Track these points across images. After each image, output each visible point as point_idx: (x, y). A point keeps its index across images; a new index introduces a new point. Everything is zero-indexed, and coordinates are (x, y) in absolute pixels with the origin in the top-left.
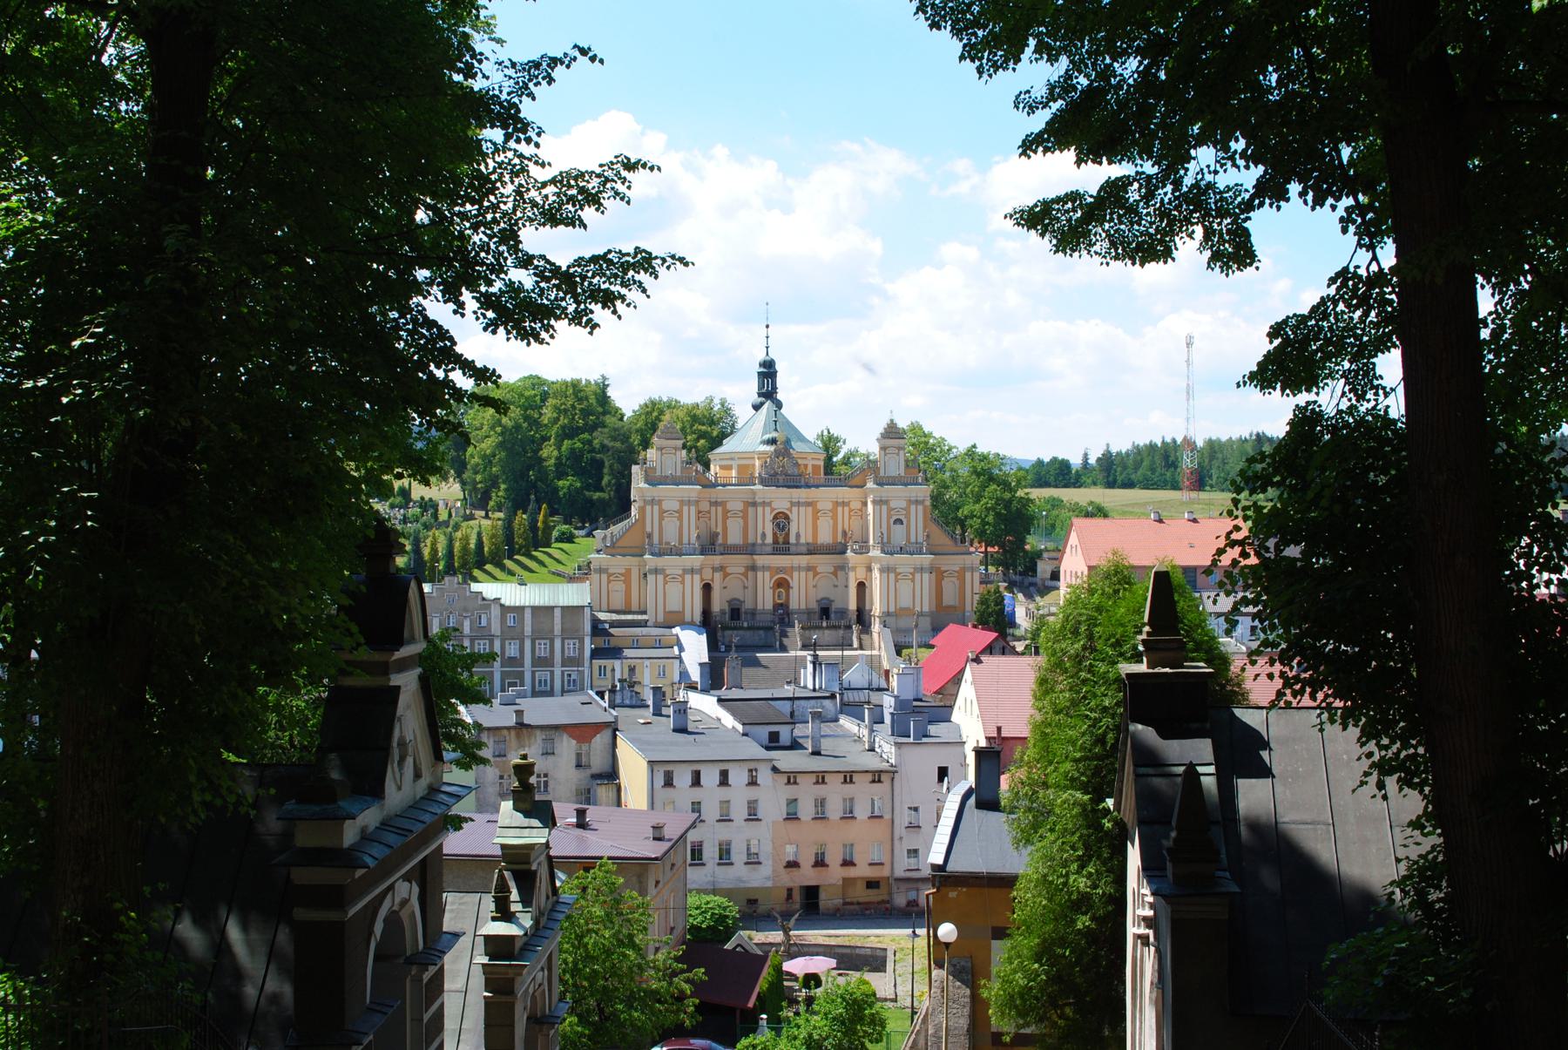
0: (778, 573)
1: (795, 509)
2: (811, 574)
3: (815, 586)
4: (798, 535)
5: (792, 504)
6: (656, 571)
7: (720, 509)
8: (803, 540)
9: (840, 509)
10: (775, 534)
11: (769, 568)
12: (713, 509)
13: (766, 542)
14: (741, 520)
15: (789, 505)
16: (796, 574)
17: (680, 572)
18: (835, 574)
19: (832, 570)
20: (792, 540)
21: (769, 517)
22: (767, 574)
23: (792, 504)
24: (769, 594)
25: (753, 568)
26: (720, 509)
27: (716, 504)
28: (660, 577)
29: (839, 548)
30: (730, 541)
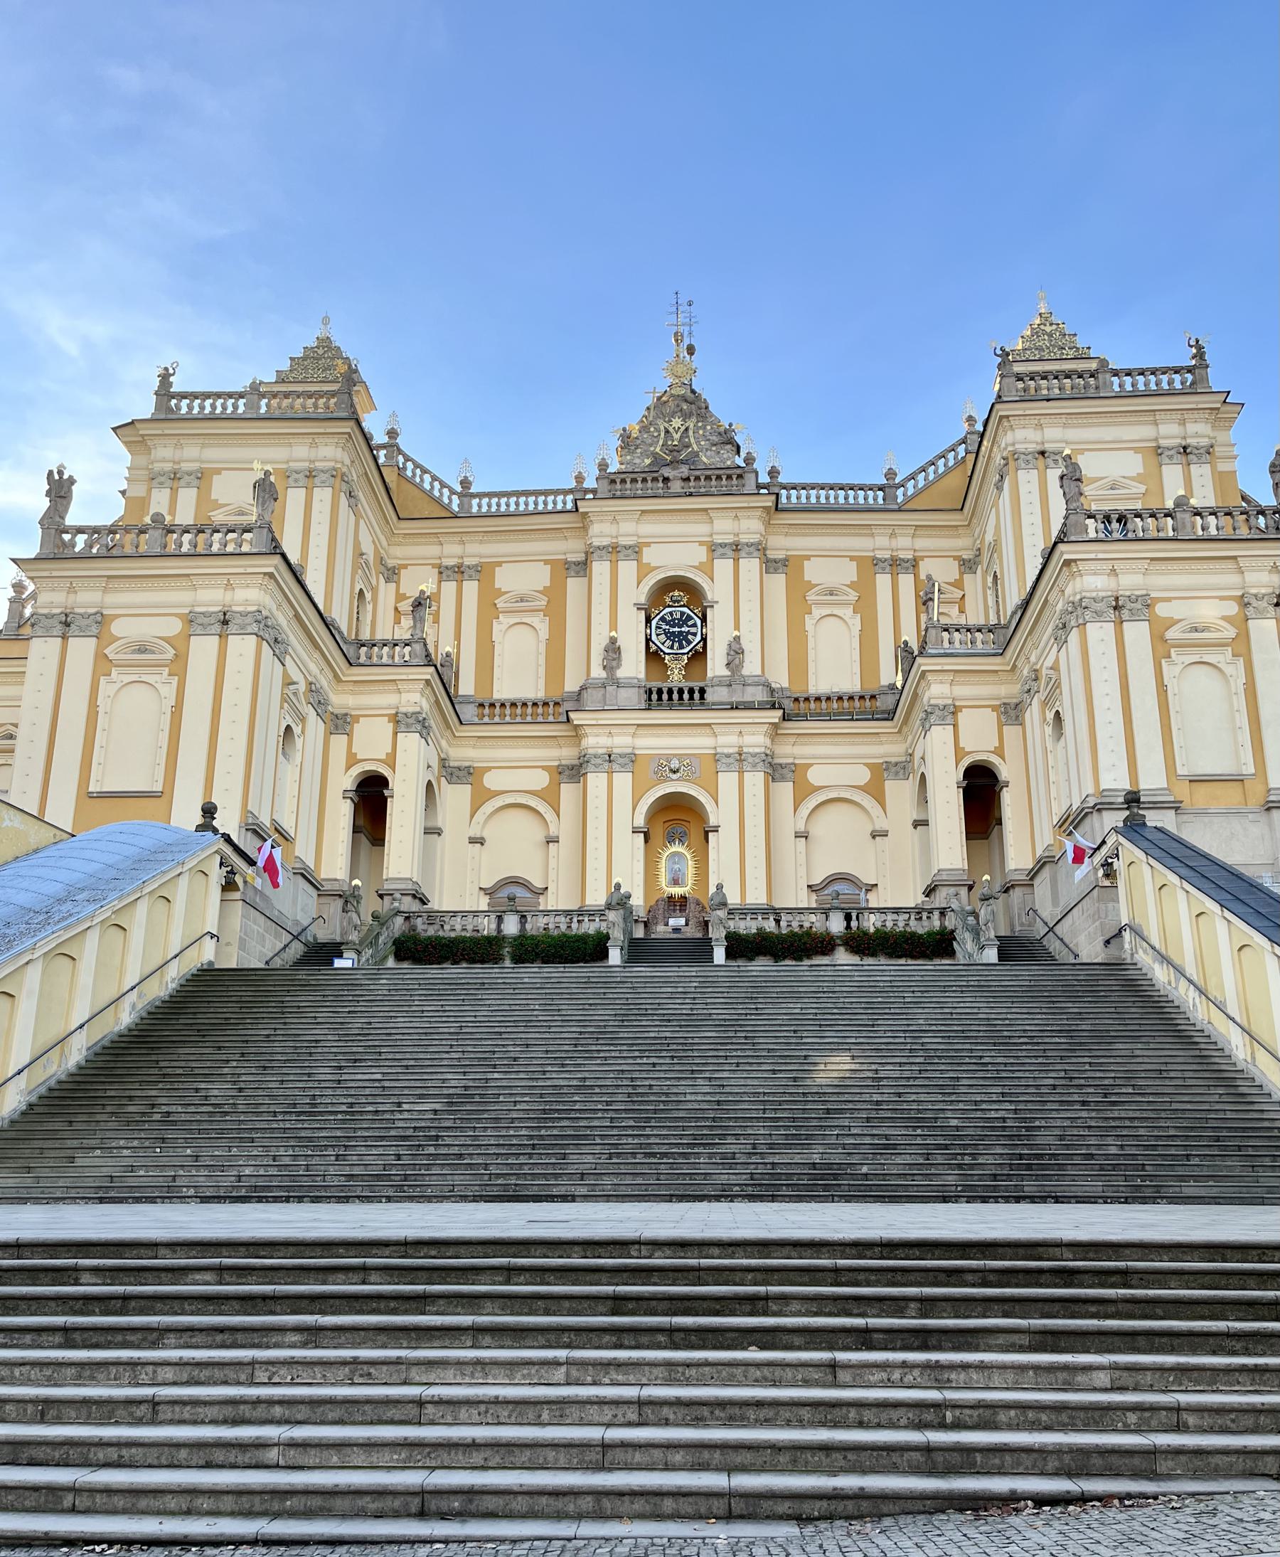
0: (664, 780)
1: (723, 567)
2: (785, 791)
3: (803, 835)
4: (736, 652)
5: (714, 549)
6: (67, 624)
7: (471, 588)
8: (751, 667)
9: (883, 581)
10: (653, 656)
11: (631, 760)
12: (449, 588)
13: (621, 673)
14: (542, 624)
15: (701, 554)
16: (727, 781)
17: (174, 627)
18: (875, 789)
19: (864, 776)
20: (716, 665)
21: (635, 592)
22: (623, 781)
23: (714, 549)
24: (630, 850)
25: (575, 772)
26: (471, 588)
27: (458, 572)
28: (82, 649)
29: (885, 702)
30: (502, 691)
